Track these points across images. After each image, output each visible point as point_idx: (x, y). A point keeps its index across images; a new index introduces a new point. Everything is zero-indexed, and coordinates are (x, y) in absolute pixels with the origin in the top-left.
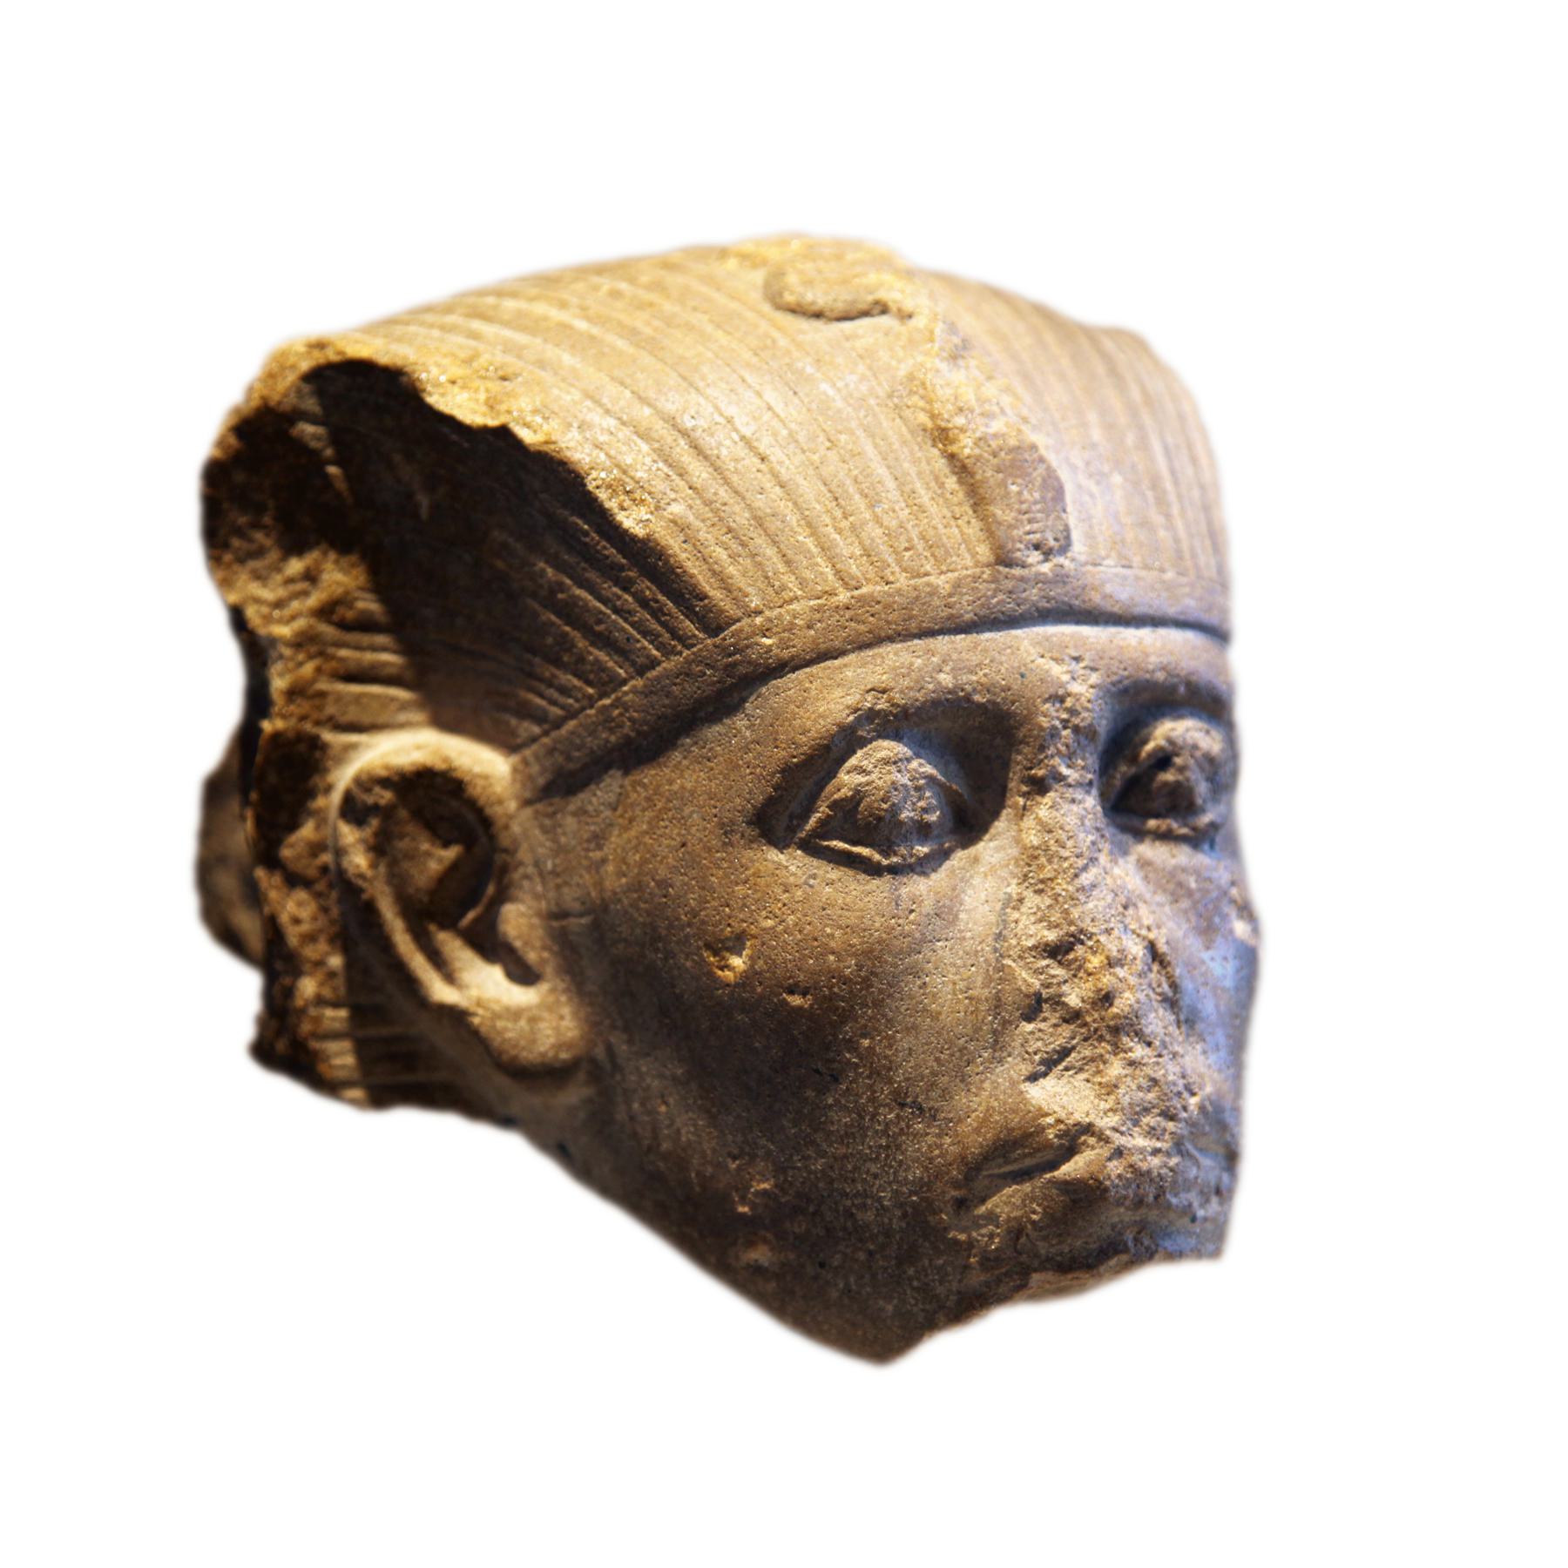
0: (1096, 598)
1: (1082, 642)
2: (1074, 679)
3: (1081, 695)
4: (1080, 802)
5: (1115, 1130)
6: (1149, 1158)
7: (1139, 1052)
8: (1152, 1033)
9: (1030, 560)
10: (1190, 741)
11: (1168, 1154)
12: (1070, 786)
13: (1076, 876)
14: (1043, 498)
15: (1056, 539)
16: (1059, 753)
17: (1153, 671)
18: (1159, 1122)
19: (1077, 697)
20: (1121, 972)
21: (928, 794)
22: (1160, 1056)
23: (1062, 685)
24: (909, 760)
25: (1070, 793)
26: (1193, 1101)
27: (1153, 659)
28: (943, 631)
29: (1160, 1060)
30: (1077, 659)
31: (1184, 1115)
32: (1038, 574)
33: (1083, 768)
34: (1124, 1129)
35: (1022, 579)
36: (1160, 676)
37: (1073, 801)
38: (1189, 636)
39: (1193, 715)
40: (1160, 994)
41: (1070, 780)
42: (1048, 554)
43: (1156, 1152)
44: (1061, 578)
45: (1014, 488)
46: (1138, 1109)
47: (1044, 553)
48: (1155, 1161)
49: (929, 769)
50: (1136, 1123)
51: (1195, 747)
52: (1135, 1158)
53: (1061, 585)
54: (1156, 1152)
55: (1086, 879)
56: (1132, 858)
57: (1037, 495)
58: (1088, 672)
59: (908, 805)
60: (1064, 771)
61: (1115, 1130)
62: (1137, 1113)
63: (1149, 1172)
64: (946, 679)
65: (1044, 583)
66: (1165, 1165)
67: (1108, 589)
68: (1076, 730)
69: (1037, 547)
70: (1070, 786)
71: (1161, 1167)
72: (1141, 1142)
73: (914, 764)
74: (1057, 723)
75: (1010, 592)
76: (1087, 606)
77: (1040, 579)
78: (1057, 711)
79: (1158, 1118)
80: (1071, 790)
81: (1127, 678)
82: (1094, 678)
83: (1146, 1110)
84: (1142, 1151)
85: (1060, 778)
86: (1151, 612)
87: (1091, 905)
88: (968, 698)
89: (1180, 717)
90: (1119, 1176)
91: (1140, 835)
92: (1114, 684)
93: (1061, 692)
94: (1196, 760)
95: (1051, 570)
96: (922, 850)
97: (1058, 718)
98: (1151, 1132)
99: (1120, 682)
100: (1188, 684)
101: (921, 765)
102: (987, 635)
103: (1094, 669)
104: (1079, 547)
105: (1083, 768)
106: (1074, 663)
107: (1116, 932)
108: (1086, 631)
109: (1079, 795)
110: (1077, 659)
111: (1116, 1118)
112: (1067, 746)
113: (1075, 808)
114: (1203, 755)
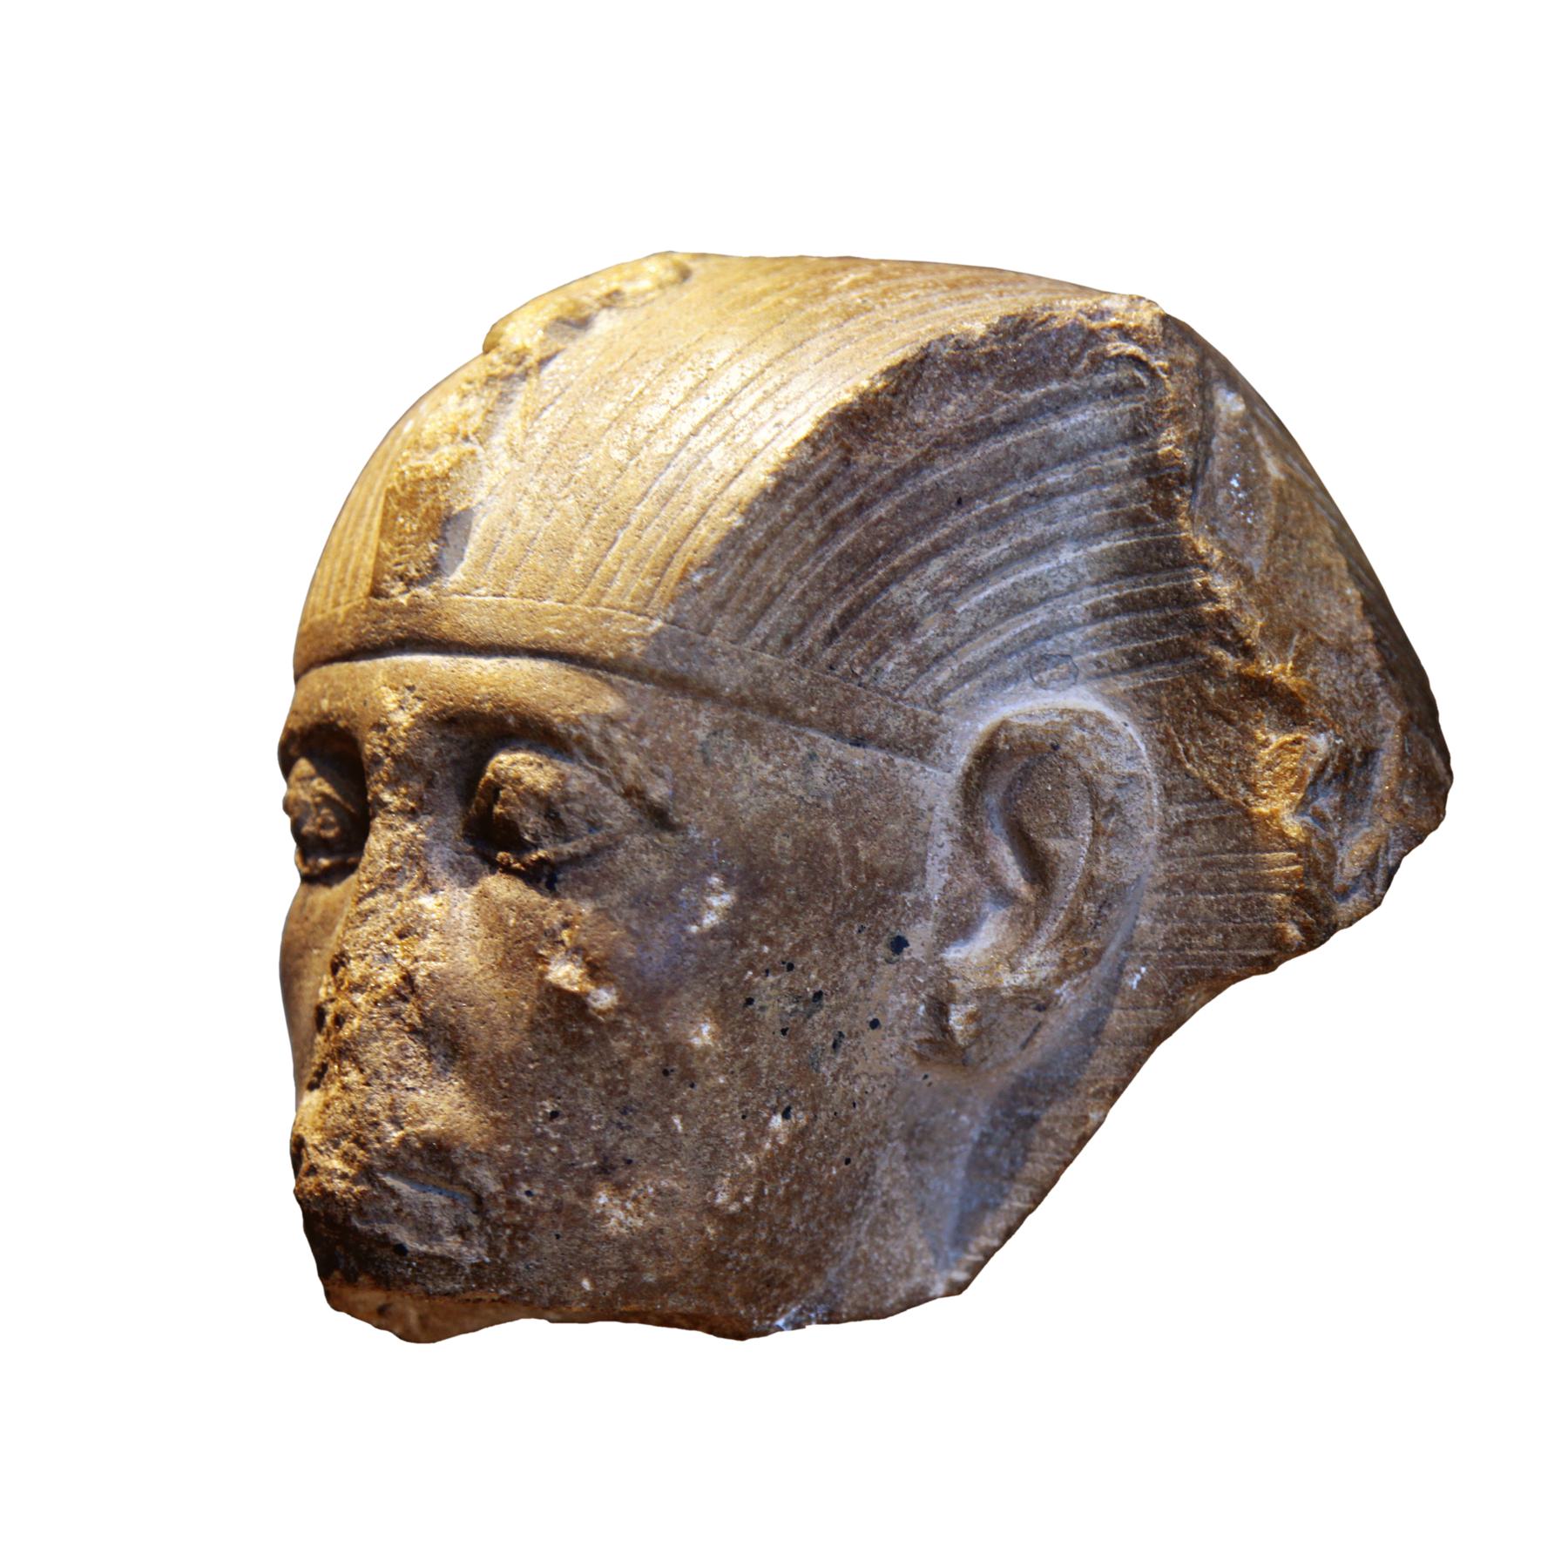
0: (445, 627)
1: (421, 670)
2: (402, 708)
3: (400, 724)
4: (397, 829)
5: (315, 1147)
6: (337, 1181)
7: (354, 1077)
8: (366, 1061)
9: (393, 592)
10: (512, 774)
11: (355, 1181)
12: (391, 812)
13: (360, 900)
14: (419, 529)
15: (418, 571)
16: (382, 780)
17: (480, 702)
18: (351, 1148)
19: (396, 726)
20: (359, 998)
21: (324, 811)
22: (367, 1084)
23: (386, 714)
24: (312, 778)
25: (390, 819)
26: (398, 1134)
27: (483, 689)
28: (330, 661)
29: (367, 1088)
30: (411, 688)
31: (377, 1146)
32: (398, 604)
33: (405, 796)
34: (322, 1148)
35: (384, 610)
36: (488, 706)
37: (390, 827)
38: (543, 666)
39: (530, 748)
40: (410, 1025)
41: (391, 807)
42: (410, 583)
43: (344, 1176)
44: (416, 607)
45: (401, 520)
46: (337, 1132)
47: (407, 585)
48: (341, 1185)
49: (326, 788)
50: (336, 1146)
51: (518, 780)
52: (323, 1178)
53: (414, 615)
54: (344, 1176)
55: (369, 903)
56: (476, 890)
57: (415, 527)
58: (416, 701)
59: (309, 821)
60: (386, 797)
61: (315, 1147)
62: (337, 1136)
63: (332, 1194)
64: (325, 704)
65: (400, 613)
66: (349, 1191)
67: (463, 618)
68: (394, 757)
69: (401, 578)
70: (391, 812)
71: (345, 1192)
72: (337, 1164)
73: (315, 783)
74: (379, 751)
75: (375, 622)
76: (435, 635)
77: (398, 609)
78: (381, 739)
79: (352, 1145)
80: (390, 816)
81: (452, 708)
82: (419, 707)
83: (344, 1135)
84: (331, 1172)
85: (384, 805)
86: (498, 640)
87: (360, 930)
88: (334, 724)
89: (516, 750)
90: (311, 1193)
91: (494, 866)
92: (436, 713)
93: (383, 720)
94: (518, 794)
95: (409, 601)
96: (324, 862)
97: (381, 746)
98: (347, 1158)
99: (444, 711)
100: (516, 714)
101: (320, 784)
102: (363, 664)
103: (420, 699)
104: (457, 577)
105: (405, 796)
106: (407, 692)
107: (368, 959)
108: (437, 663)
109: (397, 821)
110: (411, 688)
111: (319, 1137)
112: (388, 774)
113: (390, 834)
114: (525, 790)
